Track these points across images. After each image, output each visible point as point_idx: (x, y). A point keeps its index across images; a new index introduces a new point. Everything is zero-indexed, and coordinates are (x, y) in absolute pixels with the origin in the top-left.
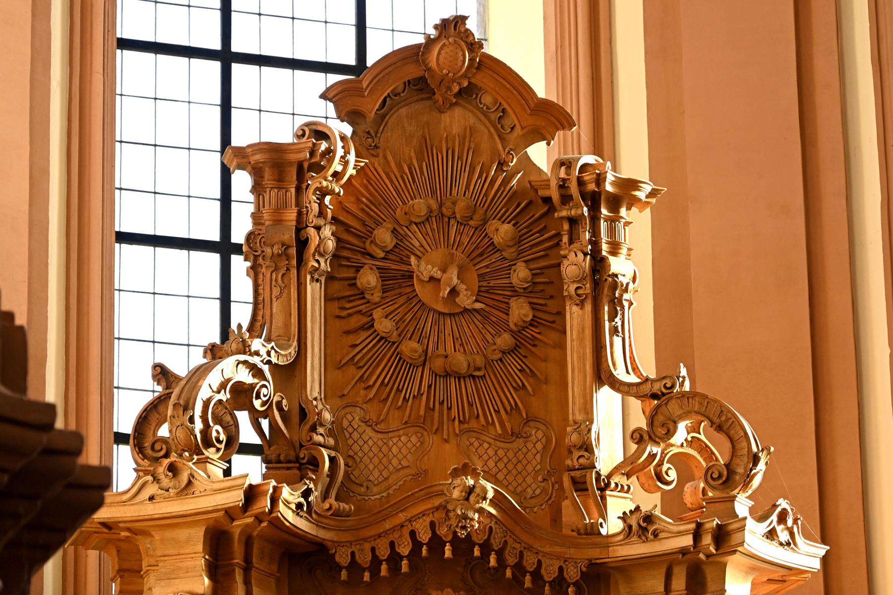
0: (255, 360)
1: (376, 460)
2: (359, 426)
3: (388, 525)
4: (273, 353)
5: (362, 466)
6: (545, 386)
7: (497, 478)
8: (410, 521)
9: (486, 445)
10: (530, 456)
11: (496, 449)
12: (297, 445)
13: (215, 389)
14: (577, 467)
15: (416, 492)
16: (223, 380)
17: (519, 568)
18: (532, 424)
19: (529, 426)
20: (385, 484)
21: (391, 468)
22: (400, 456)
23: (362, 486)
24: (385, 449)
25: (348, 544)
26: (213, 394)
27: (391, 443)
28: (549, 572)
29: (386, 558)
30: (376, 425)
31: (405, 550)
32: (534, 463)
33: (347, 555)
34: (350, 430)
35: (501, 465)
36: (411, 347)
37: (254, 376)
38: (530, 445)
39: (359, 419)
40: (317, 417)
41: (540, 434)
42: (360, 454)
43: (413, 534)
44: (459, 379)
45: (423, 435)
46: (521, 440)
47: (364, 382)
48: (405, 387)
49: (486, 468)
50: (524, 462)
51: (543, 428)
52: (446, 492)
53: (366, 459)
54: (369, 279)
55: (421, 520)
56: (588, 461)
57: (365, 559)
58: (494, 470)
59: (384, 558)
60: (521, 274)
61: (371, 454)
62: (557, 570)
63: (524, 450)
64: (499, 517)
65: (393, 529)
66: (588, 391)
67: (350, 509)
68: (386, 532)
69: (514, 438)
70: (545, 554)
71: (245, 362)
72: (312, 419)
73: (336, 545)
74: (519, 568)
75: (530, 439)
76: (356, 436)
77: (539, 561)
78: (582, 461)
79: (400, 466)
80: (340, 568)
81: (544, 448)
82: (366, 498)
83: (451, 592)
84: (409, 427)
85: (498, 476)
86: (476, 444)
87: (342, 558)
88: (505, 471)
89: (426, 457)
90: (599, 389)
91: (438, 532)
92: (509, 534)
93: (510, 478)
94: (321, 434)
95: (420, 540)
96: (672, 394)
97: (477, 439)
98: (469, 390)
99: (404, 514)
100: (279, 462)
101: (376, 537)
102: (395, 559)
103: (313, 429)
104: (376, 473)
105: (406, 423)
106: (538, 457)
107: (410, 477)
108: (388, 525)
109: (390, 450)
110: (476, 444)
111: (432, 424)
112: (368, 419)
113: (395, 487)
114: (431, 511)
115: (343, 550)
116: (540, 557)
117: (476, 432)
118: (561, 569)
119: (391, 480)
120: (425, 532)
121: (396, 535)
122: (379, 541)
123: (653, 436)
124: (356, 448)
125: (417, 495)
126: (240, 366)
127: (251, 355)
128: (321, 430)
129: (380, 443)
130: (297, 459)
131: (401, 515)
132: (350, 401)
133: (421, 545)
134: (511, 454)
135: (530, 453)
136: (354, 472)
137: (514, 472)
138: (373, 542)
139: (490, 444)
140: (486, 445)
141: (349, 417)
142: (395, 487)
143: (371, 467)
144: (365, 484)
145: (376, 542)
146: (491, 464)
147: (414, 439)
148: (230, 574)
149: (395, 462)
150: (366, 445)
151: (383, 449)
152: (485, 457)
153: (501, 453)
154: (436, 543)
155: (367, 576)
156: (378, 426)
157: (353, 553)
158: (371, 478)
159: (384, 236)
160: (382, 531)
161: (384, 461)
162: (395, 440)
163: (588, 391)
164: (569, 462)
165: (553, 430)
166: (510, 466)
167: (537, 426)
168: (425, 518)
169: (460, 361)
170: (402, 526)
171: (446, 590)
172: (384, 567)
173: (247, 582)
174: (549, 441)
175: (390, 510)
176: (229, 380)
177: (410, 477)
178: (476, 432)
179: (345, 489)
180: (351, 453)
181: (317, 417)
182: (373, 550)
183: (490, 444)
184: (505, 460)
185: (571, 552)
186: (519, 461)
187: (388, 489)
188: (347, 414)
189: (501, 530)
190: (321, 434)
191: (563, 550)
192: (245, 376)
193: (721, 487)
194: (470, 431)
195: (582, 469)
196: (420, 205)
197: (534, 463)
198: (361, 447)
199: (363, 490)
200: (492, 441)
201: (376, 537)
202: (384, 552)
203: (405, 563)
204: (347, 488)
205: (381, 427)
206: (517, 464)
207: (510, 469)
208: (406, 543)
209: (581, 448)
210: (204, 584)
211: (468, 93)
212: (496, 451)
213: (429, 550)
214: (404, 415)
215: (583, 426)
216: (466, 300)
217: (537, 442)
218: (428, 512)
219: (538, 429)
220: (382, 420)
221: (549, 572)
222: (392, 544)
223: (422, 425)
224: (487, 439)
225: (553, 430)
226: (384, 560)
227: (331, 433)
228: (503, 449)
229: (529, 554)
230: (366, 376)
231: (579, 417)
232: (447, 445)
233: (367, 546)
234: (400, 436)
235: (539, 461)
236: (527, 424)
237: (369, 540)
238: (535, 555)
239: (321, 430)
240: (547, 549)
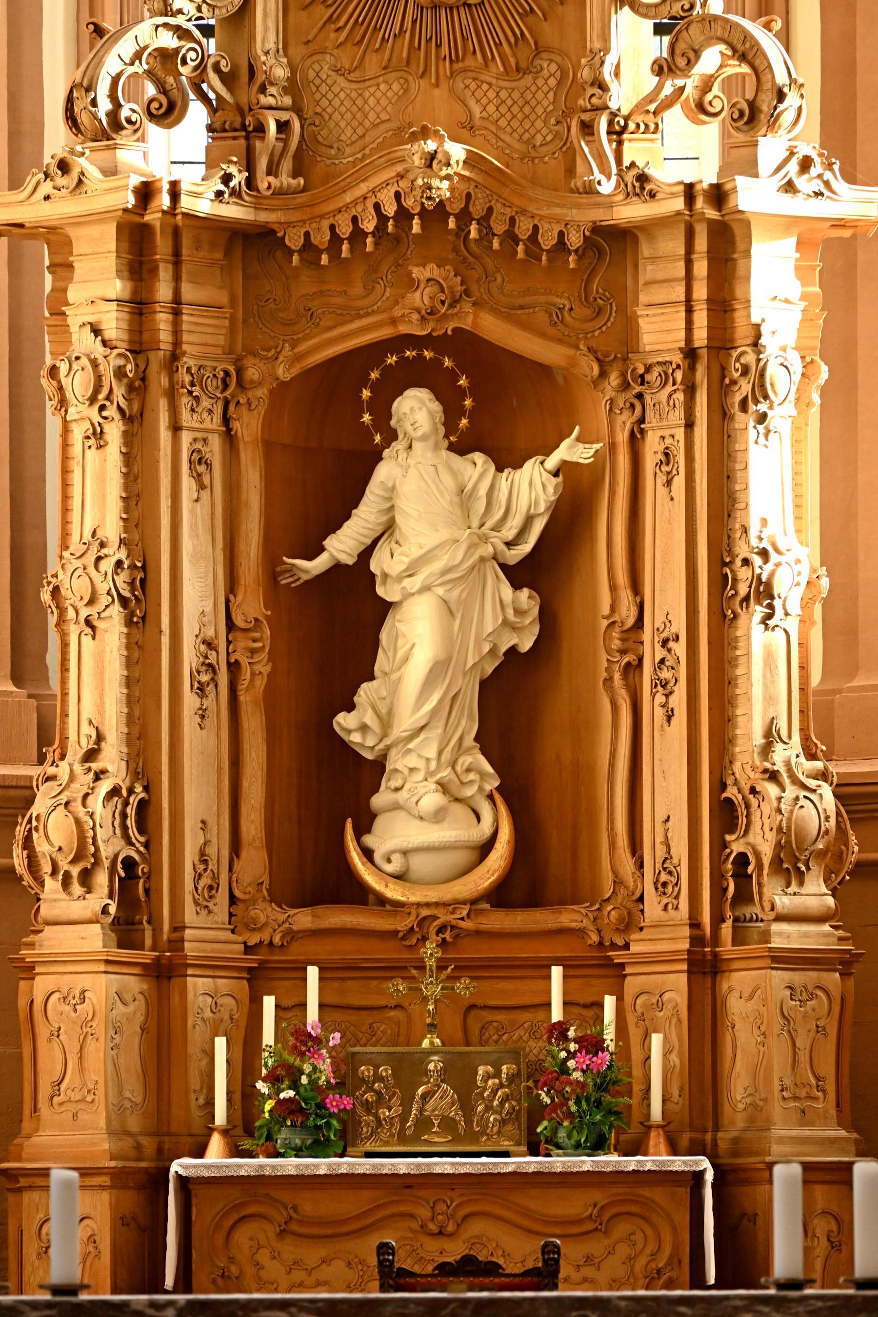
0: (180, 20)
1: (348, 116)
2: (328, 76)
3: (348, 198)
4: (204, 7)
5: (331, 124)
6: (560, 7)
7: (498, 125)
8: (373, 191)
9: (485, 87)
10: (540, 95)
11: (498, 90)
12: (246, 109)
13: (127, 61)
14: (589, 107)
15: (375, 160)
16: (138, 48)
17: (511, 237)
18: (544, 55)
19: (541, 59)
20: (361, 143)
21: (367, 123)
22: (378, 109)
23: (331, 147)
24: (360, 102)
25: (301, 224)
26: (125, 67)
27: (367, 94)
29: (347, 235)
30: (349, 73)
31: (369, 225)
32: (545, 103)
33: (300, 237)
34: (317, 81)
35: (503, 109)
37: (180, 38)
38: (540, 82)
39: (329, 68)
40: (264, 76)
41: (553, 67)
42: (329, 110)
43: (377, 207)
44: (451, 9)
45: (406, 80)
46: (530, 76)
47: (334, 23)
48: (384, 26)
49: (484, 114)
50: (533, 103)
51: (558, 58)
52: (407, 158)
53: (337, 116)
55: (386, 190)
56: (601, 101)
57: (322, 238)
58: (496, 116)
59: (344, 237)
61: (343, 109)
62: (556, 236)
63: (533, 88)
64: (480, 181)
65: (355, 202)
66: (606, 13)
67: (299, 184)
68: (347, 207)
69: (521, 75)
70: (542, 218)
71: (165, 25)
72: (260, 78)
73: (285, 226)
74: (511, 237)
75: (542, 74)
76: (324, 88)
77: (536, 228)
78: (594, 100)
79: (378, 121)
80: (290, 252)
81: (559, 83)
82: (337, 162)
83: (435, 267)
84: (391, 72)
85: (500, 123)
86: (473, 86)
87: (294, 240)
88: (509, 116)
89: (410, 107)
90: (621, 9)
91: (404, 204)
92: (495, 197)
93: (515, 124)
94: (272, 95)
95: (385, 213)
96: (691, 18)
97: (474, 79)
98: (464, 22)
99: (366, 184)
100: (225, 131)
101: (336, 213)
102: (358, 235)
103: (263, 90)
104: (349, 132)
105: (385, 68)
106: (551, 95)
107: (391, 133)
108: (348, 198)
109: (366, 102)
110: (473, 86)
111: (418, 66)
112: (339, 67)
113: (371, 146)
114: (395, 180)
115: (294, 231)
116: (536, 222)
117: (472, 71)
118: (561, 234)
119: (367, 139)
120: (391, 203)
121: (360, 208)
122: (339, 216)
123: (673, 67)
124: (324, 103)
125: (376, 162)
126: (160, 29)
127: (173, 15)
128: (272, 90)
129: (354, 95)
130: (244, 127)
131: (362, 185)
132: (317, 47)
133: (387, 219)
134: (516, 95)
135: (540, 91)
136: (321, 133)
137: (520, 116)
138: (331, 219)
139: (490, 84)
140: (485, 87)
141: (317, 67)
142: (371, 146)
143: (343, 124)
144: (335, 146)
145: (336, 218)
146: (491, 108)
147: (396, 87)
148: (154, 270)
149: (372, 116)
150: (337, 99)
151: (357, 102)
152: (484, 101)
153: (504, 94)
154: (404, 215)
155: (324, 259)
156: (352, 75)
157: (307, 235)
158: (343, 137)
160: (342, 205)
161: (359, 116)
162: (372, 90)
163: (606, 13)
164: (581, 102)
165: (570, 60)
166: (515, 109)
167: (550, 57)
168: (389, 187)
170: (365, 198)
171: (428, 265)
172: (345, 247)
173: (177, 278)
174: (564, 73)
175: (348, 180)
176: (146, 47)
177: (391, 133)
178: (472, 71)
179: (311, 153)
180: (319, 110)
181: (264, 76)
182: (332, 228)
183: (490, 84)
184: (509, 102)
185: (574, 214)
186: (527, 103)
187: (364, 149)
188: (314, 63)
189: (484, 195)
190: (272, 95)
191: (564, 211)
192: (168, 40)
193: (745, 128)
194: (465, 70)
195: (594, 110)
197: (545, 103)
198: (330, 102)
199: (333, 152)
200: (494, 81)
201: (336, 213)
202: (345, 230)
203: (369, 240)
204: (313, 151)
205: (353, 76)
206: (523, 106)
207: (515, 113)
208: (370, 217)
209: (592, 84)
210: (115, 288)
212: (498, 93)
213: (396, 226)
214: (383, 59)
215: (597, 58)
217: (549, 77)
218: (391, 181)
219: (551, 61)
220: (356, 68)
222: (355, 220)
223: (406, 69)
224: (488, 79)
225: (570, 60)
226: (346, 239)
227: (286, 91)
228: (506, 89)
229: (522, 219)
230: (335, 16)
231: (597, 45)
232: (437, 92)
233: (325, 224)
234: (378, 85)
235: (552, 101)
236: (538, 56)
237: (327, 216)
238: (530, 220)
239: (272, 90)
240: (544, 212)
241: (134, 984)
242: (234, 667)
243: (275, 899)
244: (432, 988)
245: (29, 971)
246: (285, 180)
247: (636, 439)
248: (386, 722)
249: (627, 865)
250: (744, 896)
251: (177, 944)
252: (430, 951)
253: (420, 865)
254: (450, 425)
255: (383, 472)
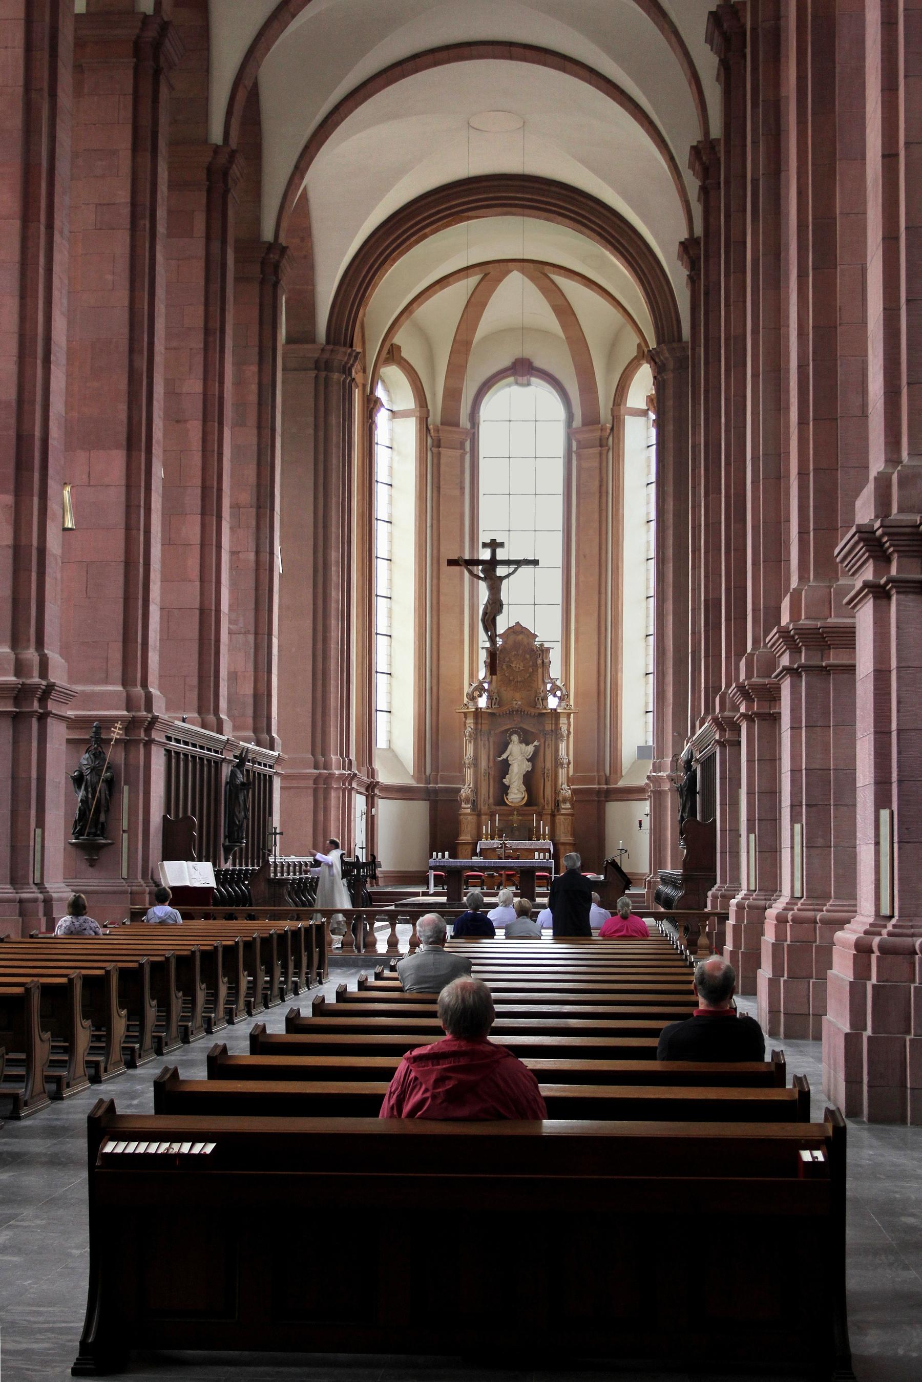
17: (527, 714)
28: (532, 714)
36: (511, 678)
54: (504, 667)
60: (531, 663)
74: (527, 714)
154: (513, 711)
159: (507, 659)
169: (519, 679)
196: (513, 653)
211: (522, 632)
216: (521, 668)
221: (532, 714)
241: (475, 817)
242: (489, 774)
243: (494, 805)
244: (515, 817)
245: (460, 814)
246: (496, 706)
247: (545, 742)
248: (510, 781)
249: (542, 801)
250: (558, 805)
251: (480, 811)
252: (515, 813)
253: (516, 801)
254: (519, 739)
255: (510, 746)
